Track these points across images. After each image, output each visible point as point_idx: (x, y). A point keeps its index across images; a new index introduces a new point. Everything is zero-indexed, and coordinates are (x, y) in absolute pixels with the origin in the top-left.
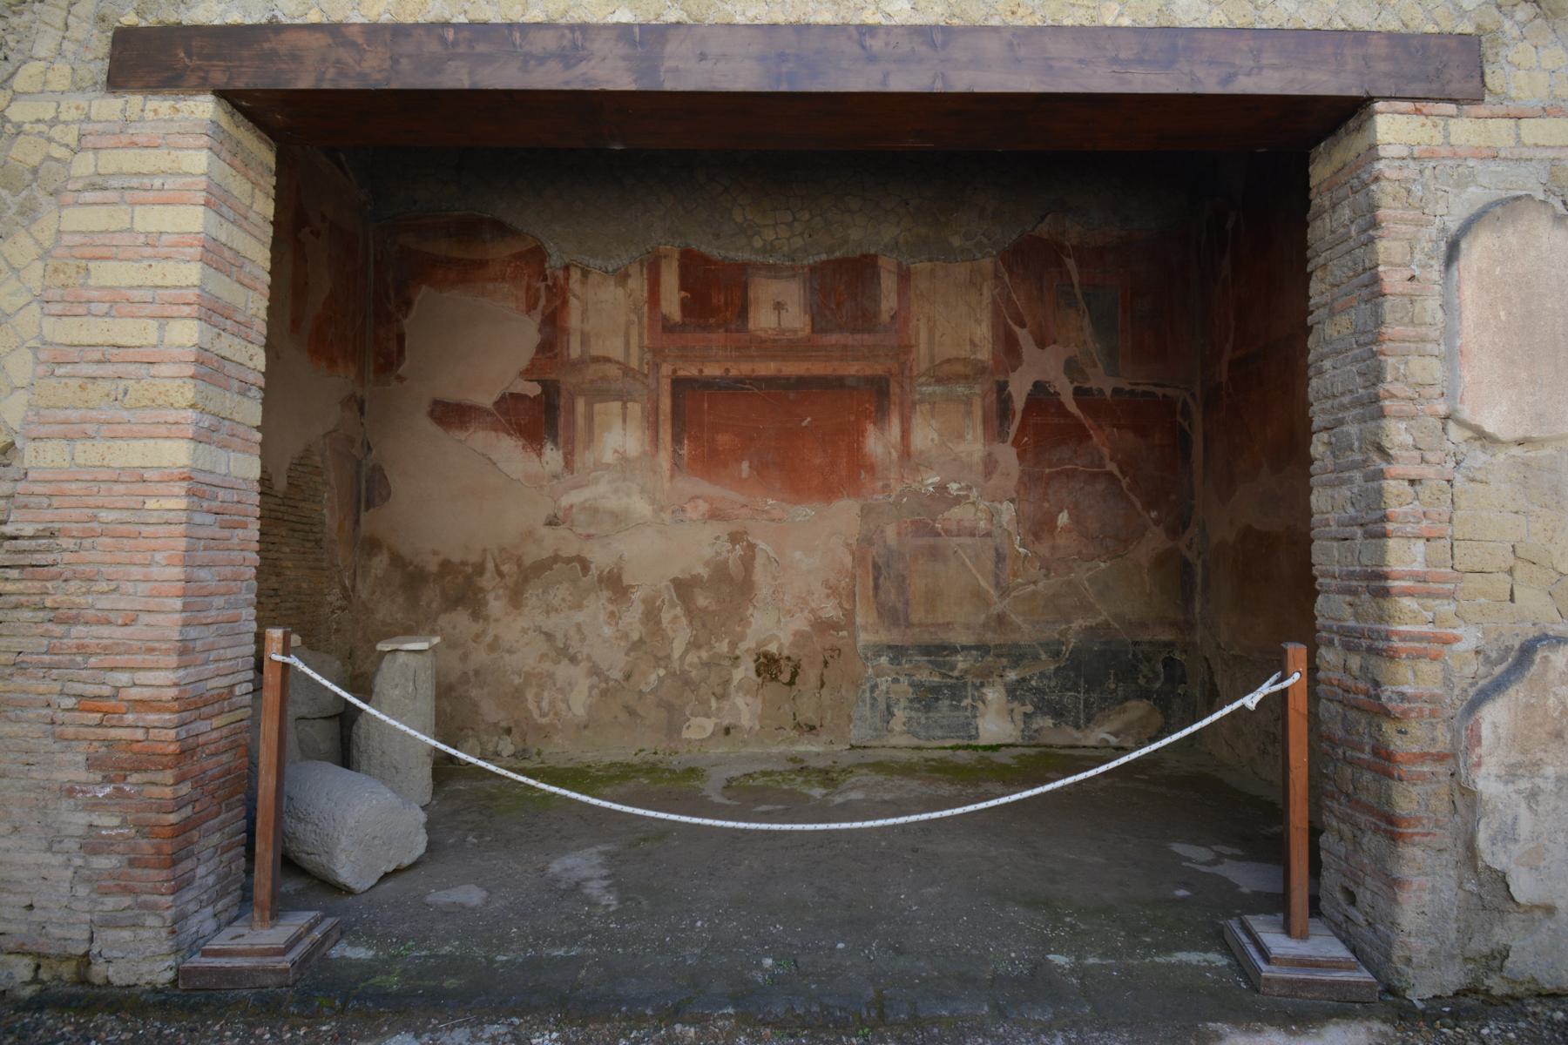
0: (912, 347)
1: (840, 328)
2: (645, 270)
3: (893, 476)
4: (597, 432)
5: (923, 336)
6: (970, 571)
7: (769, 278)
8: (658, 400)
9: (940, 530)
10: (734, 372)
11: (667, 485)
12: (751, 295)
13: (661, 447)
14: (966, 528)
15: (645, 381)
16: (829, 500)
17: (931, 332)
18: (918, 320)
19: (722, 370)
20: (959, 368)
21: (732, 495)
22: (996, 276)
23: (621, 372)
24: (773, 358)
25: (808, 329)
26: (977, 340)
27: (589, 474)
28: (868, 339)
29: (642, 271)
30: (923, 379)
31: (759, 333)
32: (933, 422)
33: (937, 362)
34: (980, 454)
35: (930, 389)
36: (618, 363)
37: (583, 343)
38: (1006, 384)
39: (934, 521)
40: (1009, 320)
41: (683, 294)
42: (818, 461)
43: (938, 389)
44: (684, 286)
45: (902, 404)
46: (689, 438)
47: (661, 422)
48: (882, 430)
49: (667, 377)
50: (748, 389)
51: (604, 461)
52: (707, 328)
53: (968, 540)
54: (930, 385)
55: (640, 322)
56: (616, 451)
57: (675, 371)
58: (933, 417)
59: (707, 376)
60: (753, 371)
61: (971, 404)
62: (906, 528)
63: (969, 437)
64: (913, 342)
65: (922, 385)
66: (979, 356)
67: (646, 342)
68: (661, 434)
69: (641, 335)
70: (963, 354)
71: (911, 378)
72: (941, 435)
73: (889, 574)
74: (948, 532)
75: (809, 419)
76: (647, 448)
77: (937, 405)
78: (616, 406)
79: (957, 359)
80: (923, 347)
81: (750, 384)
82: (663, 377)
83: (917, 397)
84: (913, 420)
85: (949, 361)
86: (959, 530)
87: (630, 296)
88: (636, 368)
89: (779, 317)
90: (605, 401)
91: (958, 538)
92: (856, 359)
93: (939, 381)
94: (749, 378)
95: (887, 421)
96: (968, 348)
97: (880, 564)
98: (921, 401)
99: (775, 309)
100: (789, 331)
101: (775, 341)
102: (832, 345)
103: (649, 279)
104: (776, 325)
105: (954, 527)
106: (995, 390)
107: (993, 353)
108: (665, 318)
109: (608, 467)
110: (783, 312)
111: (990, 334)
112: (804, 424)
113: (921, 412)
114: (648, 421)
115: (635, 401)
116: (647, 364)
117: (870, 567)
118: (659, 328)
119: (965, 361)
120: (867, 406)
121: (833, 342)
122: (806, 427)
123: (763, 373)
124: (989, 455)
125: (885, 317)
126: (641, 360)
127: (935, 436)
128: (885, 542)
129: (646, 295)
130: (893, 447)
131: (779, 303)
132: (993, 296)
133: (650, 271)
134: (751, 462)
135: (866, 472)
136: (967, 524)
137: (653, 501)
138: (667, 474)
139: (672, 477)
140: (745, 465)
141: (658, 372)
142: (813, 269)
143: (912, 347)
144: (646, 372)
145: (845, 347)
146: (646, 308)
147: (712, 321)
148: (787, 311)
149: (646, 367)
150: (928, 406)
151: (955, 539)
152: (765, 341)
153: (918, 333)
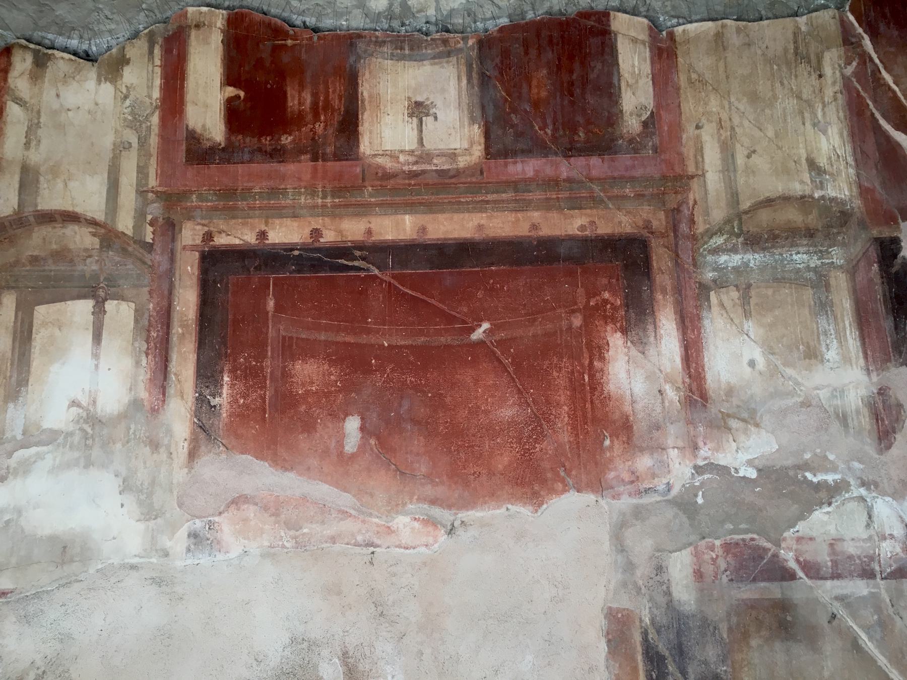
0: (693, 177)
1: (539, 148)
2: (157, 51)
3: (670, 442)
4: (36, 362)
5: (712, 157)
6: (873, 661)
7: (402, 58)
8: (170, 293)
9: (792, 564)
10: (329, 237)
11: (180, 475)
12: (365, 90)
13: (171, 391)
14: (850, 557)
15: (148, 258)
16: (536, 499)
17: (727, 151)
18: (698, 127)
19: (307, 231)
20: (793, 215)
21: (322, 490)
22: (848, 40)
23: (97, 241)
24: (410, 207)
25: (478, 151)
26: (822, 162)
27: (10, 455)
28: (597, 165)
29: (151, 52)
30: (719, 240)
31: (380, 160)
32: (749, 326)
33: (746, 205)
34: (863, 392)
35: (736, 260)
36: (93, 223)
37: (22, 186)
38: (895, 242)
39: (778, 545)
40: (883, 122)
41: (231, 91)
42: (508, 412)
43: (754, 259)
44: (230, 79)
45: (678, 290)
46: (233, 371)
47: (174, 339)
48: (641, 344)
49: (193, 248)
50: (359, 269)
51: (47, 424)
52: (278, 154)
53: (859, 588)
54: (734, 250)
55: (143, 142)
56: (74, 403)
57: (208, 237)
58: (747, 315)
59: (275, 244)
60: (369, 232)
61: (827, 286)
62: (714, 560)
63: (832, 354)
64: (691, 169)
65: (716, 251)
66: (831, 192)
67: (153, 182)
68: (173, 366)
69: (142, 171)
70: (797, 188)
71: (694, 238)
72: (770, 351)
73: (684, 673)
74: (813, 570)
75: (486, 326)
76: (143, 394)
77: (753, 293)
78: (82, 308)
79: (786, 199)
80: (713, 179)
81: (364, 259)
82: (184, 248)
83: (710, 275)
84: (706, 323)
85: (769, 202)
86: (835, 563)
87: (126, 97)
88: (129, 232)
89: (420, 131)
90: (62, 299)
91: (836, 582)
92: (576, 204)
93: (753, 242)
94: (360, 246)
95: (650, 327)
96: (806, 177)
97: (662, 648)
98: (720, 284)
99: (411, 115)
100: (442, 155)
101: (414, 175)
102: (525, 180)
103: (164, 67)
104: (414, 146)
105: (824, 558)
106: (873, 254)
107: (860, 186)
108: (193, 137)
109: (52, 437)
110: (428, 121)
111: (849, 148)
112: (478, 334)
113: (722, 305)
114: (147, 341)
115: (121, 298)
116: (151, 224)
117: (640, 658)
118: (181, 156)
119: (804, 202)
120: (606, 295)
121: (530, 173)
122: (481, 343)
123: (389, 237)
124: (882, 392)
125: (632, 124)
126: (140, 215)
127: (757, 354)
128: (668, 593)
129: (156, 94)
130: (669, 379)
131: (418, 104)
132: (843, 76)
133: (167, 51)
134: (362, 419)
135: (614, 435)
136: (851, 549)
137: (149, 513)
138: (182, 448)
139: (192, 455)
140: (352, 424)
141: (173, 240)
142: (485, 43)
143: (693, 177)
144: (149, 239)
145: (553, 183)
146: (155, 119)
147: (286, 140)
148: (436, 118)
149: (150, 229)
150: (735, 294)
151: (829, 584)
152: (394, 176)
153: (700, 150)
